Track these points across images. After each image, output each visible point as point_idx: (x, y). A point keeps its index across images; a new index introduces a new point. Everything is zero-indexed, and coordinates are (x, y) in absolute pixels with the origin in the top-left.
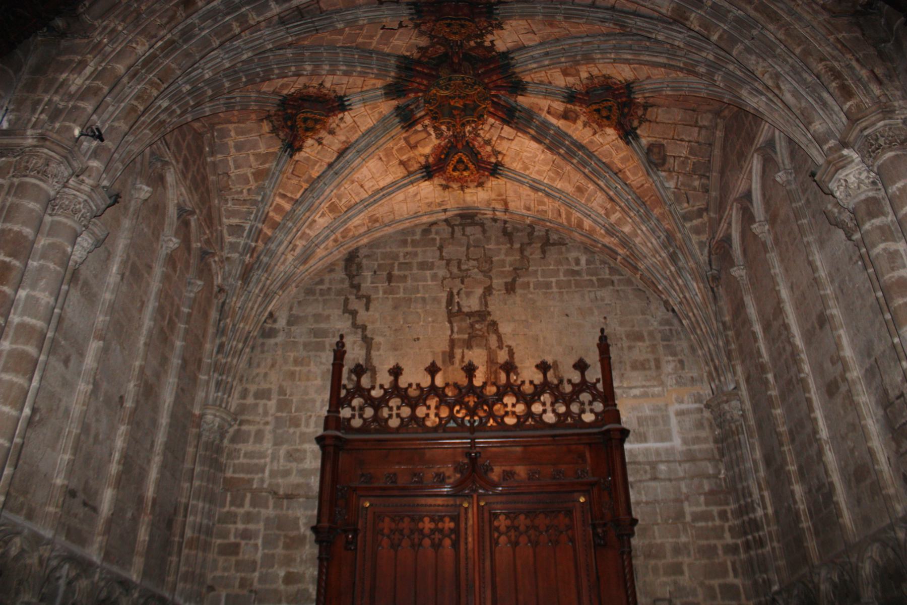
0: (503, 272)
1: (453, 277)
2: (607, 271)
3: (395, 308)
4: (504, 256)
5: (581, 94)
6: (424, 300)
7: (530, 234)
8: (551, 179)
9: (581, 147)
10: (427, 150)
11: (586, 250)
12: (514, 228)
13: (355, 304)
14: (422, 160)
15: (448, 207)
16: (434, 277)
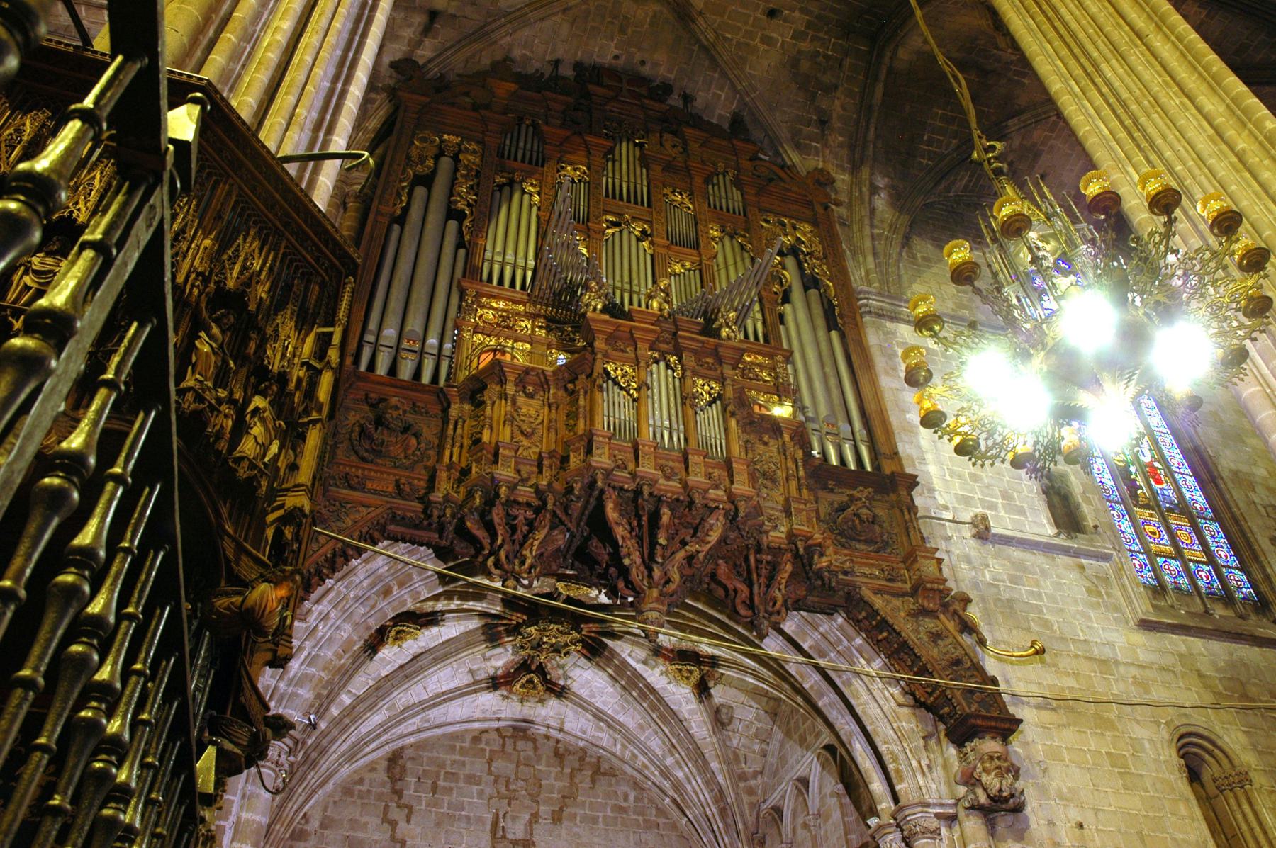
0: (551, 799)
1: (500, 797)
2: (654, 812)
3: (438, 825)
4: (553, 780)
5: (666, 649)
6: (468, 818)
7: (582, 759)
8: (614, 710)
9: (653, 691)
10: (500, 663)
11: (636, 785)
12: (566, 750)
13: (396, 814)
14: (491, 672)
15: (502, 716)
16: (481, 794)
